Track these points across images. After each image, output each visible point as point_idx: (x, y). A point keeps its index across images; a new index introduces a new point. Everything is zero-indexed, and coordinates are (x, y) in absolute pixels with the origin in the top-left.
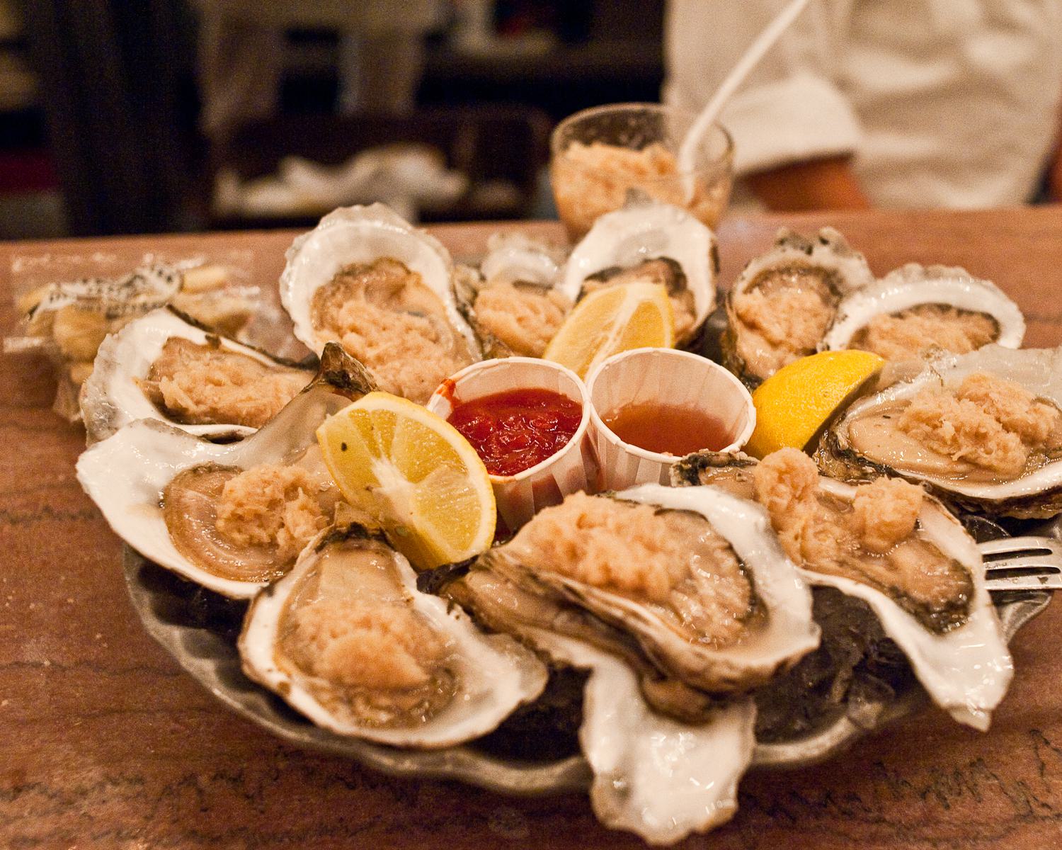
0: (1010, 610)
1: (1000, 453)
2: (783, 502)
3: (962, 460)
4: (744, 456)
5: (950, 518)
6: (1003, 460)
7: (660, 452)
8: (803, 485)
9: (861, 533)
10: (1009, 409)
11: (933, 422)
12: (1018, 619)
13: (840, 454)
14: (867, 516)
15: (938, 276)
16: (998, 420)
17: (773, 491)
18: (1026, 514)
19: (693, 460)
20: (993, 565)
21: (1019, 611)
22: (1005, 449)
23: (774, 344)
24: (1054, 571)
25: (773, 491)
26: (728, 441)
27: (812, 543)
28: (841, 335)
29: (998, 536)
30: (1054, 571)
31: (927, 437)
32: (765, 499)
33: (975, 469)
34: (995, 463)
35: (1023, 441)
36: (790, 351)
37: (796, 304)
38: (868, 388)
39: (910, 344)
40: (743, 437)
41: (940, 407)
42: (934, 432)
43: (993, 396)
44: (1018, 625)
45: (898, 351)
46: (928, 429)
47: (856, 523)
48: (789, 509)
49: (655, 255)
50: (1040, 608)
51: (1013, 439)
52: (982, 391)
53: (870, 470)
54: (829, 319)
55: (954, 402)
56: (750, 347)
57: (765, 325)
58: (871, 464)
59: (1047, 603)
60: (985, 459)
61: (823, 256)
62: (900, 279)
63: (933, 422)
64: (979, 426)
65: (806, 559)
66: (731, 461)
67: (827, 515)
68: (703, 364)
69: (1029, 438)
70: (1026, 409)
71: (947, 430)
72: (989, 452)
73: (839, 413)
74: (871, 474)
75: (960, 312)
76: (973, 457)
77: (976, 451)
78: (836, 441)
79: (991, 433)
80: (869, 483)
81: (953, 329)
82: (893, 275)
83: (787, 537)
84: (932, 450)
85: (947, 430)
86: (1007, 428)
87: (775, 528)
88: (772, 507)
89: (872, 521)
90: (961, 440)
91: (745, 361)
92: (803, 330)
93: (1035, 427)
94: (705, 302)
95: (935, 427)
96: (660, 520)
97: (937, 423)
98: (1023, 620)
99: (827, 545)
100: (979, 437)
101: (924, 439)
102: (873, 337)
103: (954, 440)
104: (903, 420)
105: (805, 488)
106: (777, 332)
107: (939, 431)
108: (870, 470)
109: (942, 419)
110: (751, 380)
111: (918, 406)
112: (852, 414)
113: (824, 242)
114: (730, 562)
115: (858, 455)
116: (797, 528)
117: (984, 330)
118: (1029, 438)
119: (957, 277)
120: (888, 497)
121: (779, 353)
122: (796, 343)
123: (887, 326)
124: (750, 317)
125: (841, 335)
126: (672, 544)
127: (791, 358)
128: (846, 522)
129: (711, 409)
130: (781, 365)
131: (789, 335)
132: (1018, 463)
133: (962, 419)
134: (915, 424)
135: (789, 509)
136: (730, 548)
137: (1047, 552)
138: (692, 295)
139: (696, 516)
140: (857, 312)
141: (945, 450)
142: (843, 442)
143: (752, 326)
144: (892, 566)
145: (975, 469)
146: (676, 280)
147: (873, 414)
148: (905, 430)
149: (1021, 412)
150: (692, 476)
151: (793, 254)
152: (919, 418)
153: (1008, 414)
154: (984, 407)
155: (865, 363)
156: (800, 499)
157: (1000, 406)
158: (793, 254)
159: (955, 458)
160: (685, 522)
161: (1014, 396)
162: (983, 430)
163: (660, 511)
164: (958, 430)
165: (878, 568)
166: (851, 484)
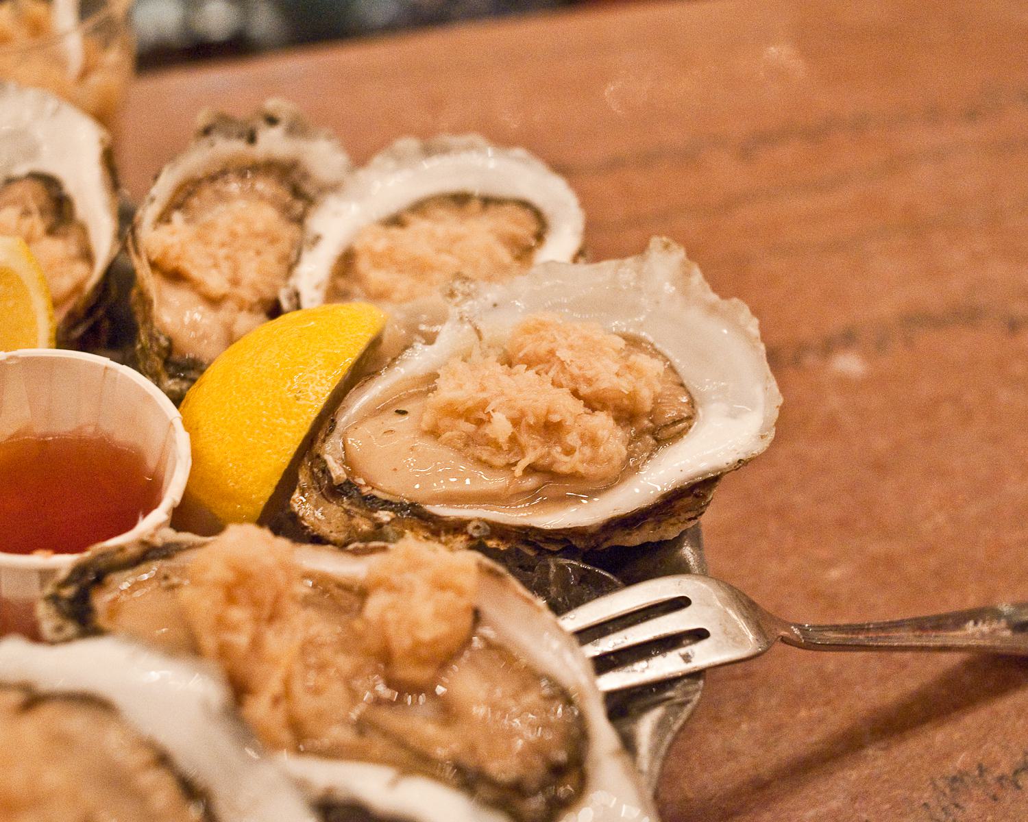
0: (645, 726)
1: (587, 451)
2: (241, 640)
3: (531, 469)
4: (170, 535)
5: (529, 601)
6: (592, 460)
7: (27, 550)
8: (269, 597)
9: (385, 657)
10: (589, 374)
11: (477, 415)
12: (661, 741)
13: (335, 491)
14: (391, 630)
15: (445, 150)
16: (575, 393)
17: (221, 624)
18: (635, 539)
19: (79, 571)
20: (609, 644)
21: (662, 725)
22: (592, 440)
23: (214, 302)
24: (699, 635)
25: (221, 624)
26: (149, 500)
27: (306, 704)
28: (313, 271)
29: (602, 589)
30: (699, 635)
31: (469, 440)
32: (209, 642)
33: (552, 482)
34: (582, 469)
35: (617, 420)
36: (241, 309)
37: (240, 229)
38: (363, 370)
39: (420, 268)
40: (172, 494)
41: (484, 389)
42: (480, 432)
43: (563, 354)
44: (663, 751)
45: (403, 283)
46: (469, 427)
47: (373, 642)
48: (256, 644)
49: (21, 170)
50: (689, 707)
51: (602, 422)
52: (543, 348)
53: (385, 516)
54: (292, 247)
55: (500, 369)
56: (174, 314)
57: (195, 273)
58: (386, 504)
59: (697, 696)
60: (565, 464)
61: (273, 143)
62: (391, 164)
63: (477, 415)
64: (548, 412)
65: (301, 737)
66: (148, 553)
67: (324, 628)
68: (94, 367)
69: (626, 415)
70: (616, 368)
71: (501, 427)
72: (569, 452)
73: (326, 421)
74: (388, 523)
75: (488, 202)
76: (547, 461)
77: (549, 454)
78: (326, 471)
79: (569, 422)
80: (384, 549)
81: (481, 234)
82: (377, 160)
83: (259, 708)
84: (480, 462)
85: (501, 427)
86: (593, 403)
87: (239, 690)
88: (224, 652)
89: (401, 642)
90: (524, 438)
91: (170, 340)
92: (256, 272)
93: (633, 396)
94: (104, 244)
95: (480, 422)
96: (31, 728)
97: (482, 416)
98: (669, 737)
99: (331, 702)
100: (550, 429)
101: (467, 445)
102: (363, 265)
103: (513, 439)
104: (427, 420)
105: (277, 599)
106: (216, 282)
107: (487, 430)
108: (385, 516)
109: (489, 409)
110: (178, 369)
111: (447, 392)
112: (343, 420)
113: (272, 121)
114: (162, 792)
115: (365, 490)
116: (274, 685)
117: (524, 228)
118: (626, 415)
119: (470, 147)
120: (419, 582)
121: (224, 314)
122: (247, 294)
123: (380, 245)
124: (171, 264)
125: (313, 271)
126: (54, 777)
127: (244, 321)
128: (359, 637)
129: (122, 435)
130: (230, 339)
131: (235, 282)
132: (617, 462)
133: (521, 404)
134: (447, 422)
135: (256, 644)
136: (163, 760)
137: (680, 603)
138: (83, 230)
139: (92, 703)
140: (336, 223)
141: (499, 460)
142: (338, 472)
143: (176, 277)
144: (448, 712)
145: (552, 482)
146: (58, 208)
147: (376, 411)
148: (434, 433)
149: (608, 376)
150: (80, 614)
151: (228, 148)
152: (453, 412)
153: (589, 381)
154: (551, 374)
155: (357, 324)
156: (272, 618)
157: (576, 371)
158: (228, 148)
159: (518, 471)
160: (77, 722)
161: (594, 348)
162: (555, 418)
163: (33, 699)
164: (516, 423)
165: (419, 723)
166: (356, 553)
